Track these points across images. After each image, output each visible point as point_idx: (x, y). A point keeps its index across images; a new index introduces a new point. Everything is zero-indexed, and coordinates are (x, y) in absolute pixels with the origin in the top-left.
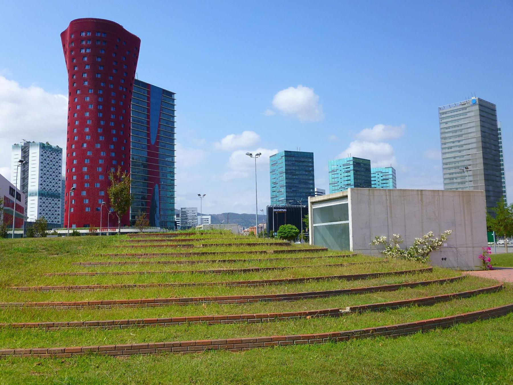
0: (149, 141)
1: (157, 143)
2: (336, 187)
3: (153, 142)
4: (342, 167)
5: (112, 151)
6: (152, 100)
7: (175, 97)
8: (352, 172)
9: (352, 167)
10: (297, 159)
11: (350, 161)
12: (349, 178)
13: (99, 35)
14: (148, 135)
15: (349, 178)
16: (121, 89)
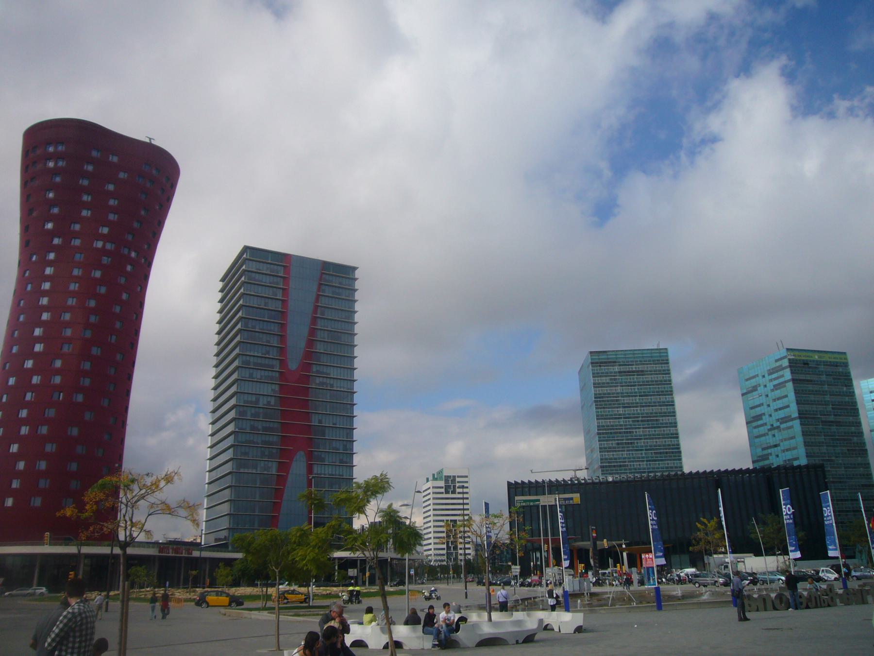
0: (283, 363)
1: (306, 366)
2: (761, 429)
3: (293, 365)
4: (767, 378)
5: (58, 372)
6: (292, 284)
7: (357, 274)
8: (790, 385)
9: (788, 374)
10: (623, 368)
11: (781, 359)
12: (785, 401)
13: (51, 149)
14: (282, 351)
15: (785, 401)
16: (99, 244)
